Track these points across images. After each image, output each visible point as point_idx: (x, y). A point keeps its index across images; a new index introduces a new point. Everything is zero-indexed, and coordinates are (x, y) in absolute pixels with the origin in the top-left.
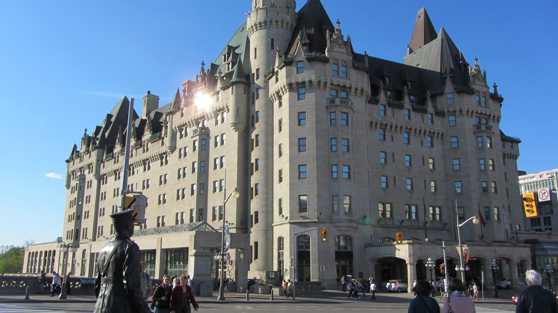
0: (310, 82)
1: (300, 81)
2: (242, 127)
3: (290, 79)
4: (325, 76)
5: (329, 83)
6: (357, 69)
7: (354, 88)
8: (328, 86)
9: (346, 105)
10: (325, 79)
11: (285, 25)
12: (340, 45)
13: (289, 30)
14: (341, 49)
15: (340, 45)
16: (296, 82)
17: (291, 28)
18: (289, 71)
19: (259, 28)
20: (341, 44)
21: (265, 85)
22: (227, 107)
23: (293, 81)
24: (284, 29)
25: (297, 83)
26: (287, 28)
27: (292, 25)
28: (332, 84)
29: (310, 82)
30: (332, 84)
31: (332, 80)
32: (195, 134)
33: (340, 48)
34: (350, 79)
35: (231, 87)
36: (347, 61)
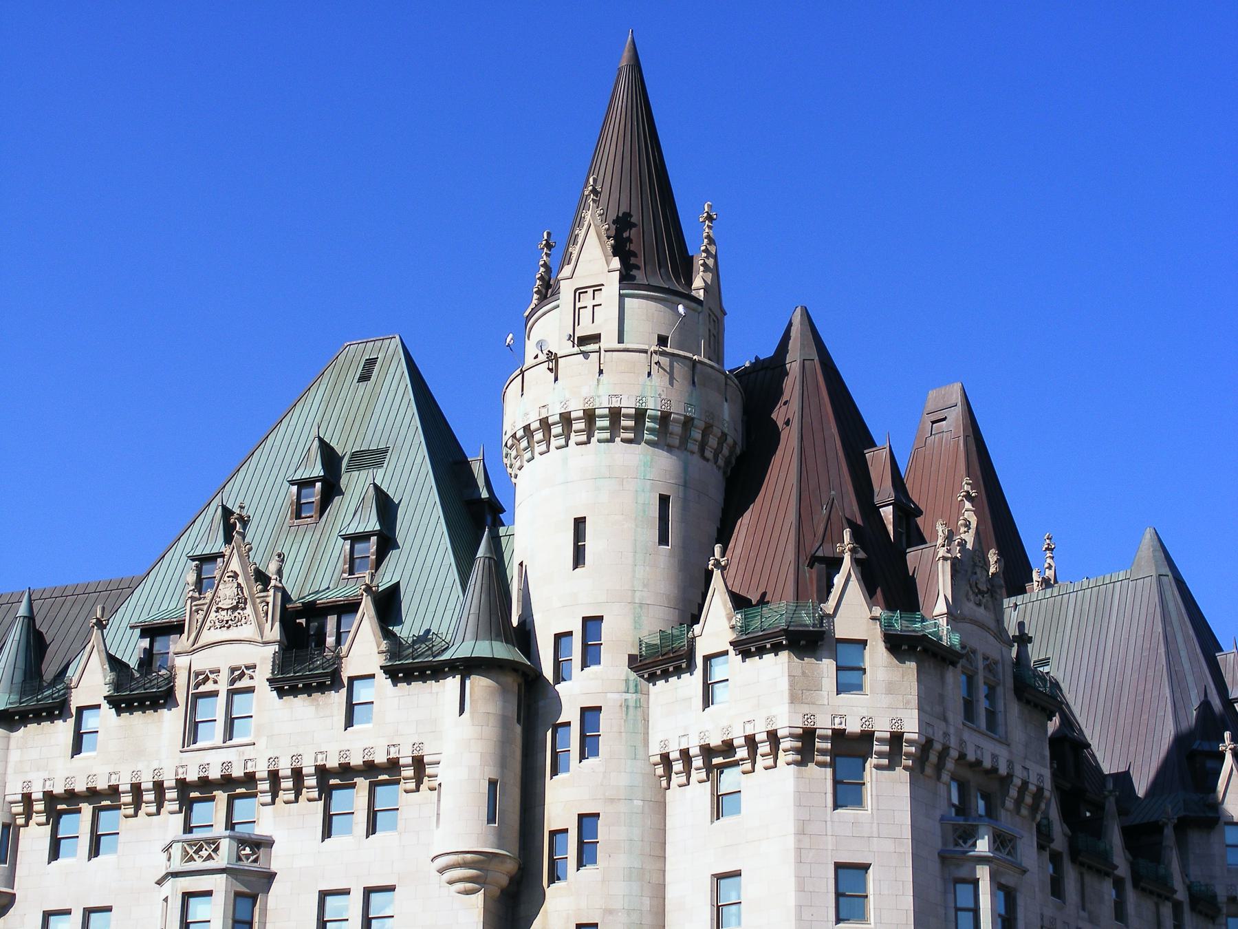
0: (896, 739)
1: (854, 727)
2: (502, 875)
3: (806, 709)
4: (945, 720)
5: (954, 754)
6: (1028, 702)
7: (1018, 782)
8: (950, 765)
9: (1008, 854)
10: (946, 734)
11: (713, 442)
12: (981, 592)
13: (719, 468)
14: (982, 610)
15: (981, 592)
16: (834, 730)
17: (728, 462)
18: (803, 673)
19: (607, 435)
20: (985, 589)
21: (632, 704)
22: (419, 763)
23: (824, 724)
24: (707, 460)
25: (839, 735)
26: (716, 454)
27: (732, 449)
28: (962, 756)
29: (896, 739)
30: (962, 756)
31: (962, 742)
32: (192, 859)
33: (979, 605)
34: (1008, 745)
35: (452, 684)
36: (996, 663)
